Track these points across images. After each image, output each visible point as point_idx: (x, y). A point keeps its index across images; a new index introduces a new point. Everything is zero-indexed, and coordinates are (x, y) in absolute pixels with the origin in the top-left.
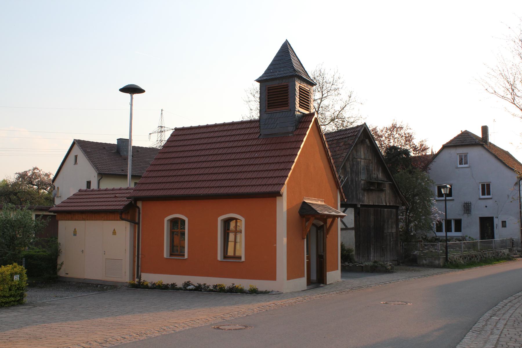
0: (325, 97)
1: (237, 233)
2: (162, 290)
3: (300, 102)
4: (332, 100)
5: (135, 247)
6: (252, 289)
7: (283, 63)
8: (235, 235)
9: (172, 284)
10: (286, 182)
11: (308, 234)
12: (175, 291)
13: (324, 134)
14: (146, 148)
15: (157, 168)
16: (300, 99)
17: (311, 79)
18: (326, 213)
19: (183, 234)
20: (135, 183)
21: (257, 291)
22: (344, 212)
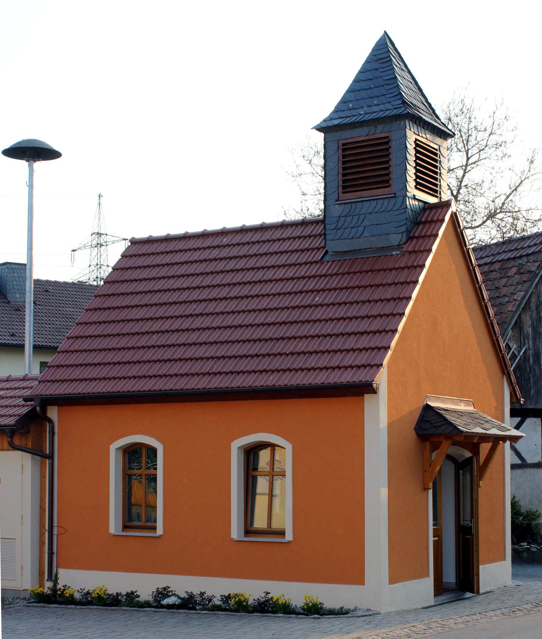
0: (474, 163)
1: (275, 478)
2: (105, 608)
3: (417, 177)
4: (490, 170)
5: (45, 510)
6: (310, 604)
7: (378, 87)
8: (269, 482)
9: (127, 592)
10: (385, 362)
11: (436, 479)
12: (136, 610)
13: (473, 249)
14: (65, 283)
15: (91, 330)
16: (417, 171)
17: (442, 123)
18: (478, 430)
19: (154, 479)
20: (41, 362)
21: (321, 608)
22: (517, 427)
